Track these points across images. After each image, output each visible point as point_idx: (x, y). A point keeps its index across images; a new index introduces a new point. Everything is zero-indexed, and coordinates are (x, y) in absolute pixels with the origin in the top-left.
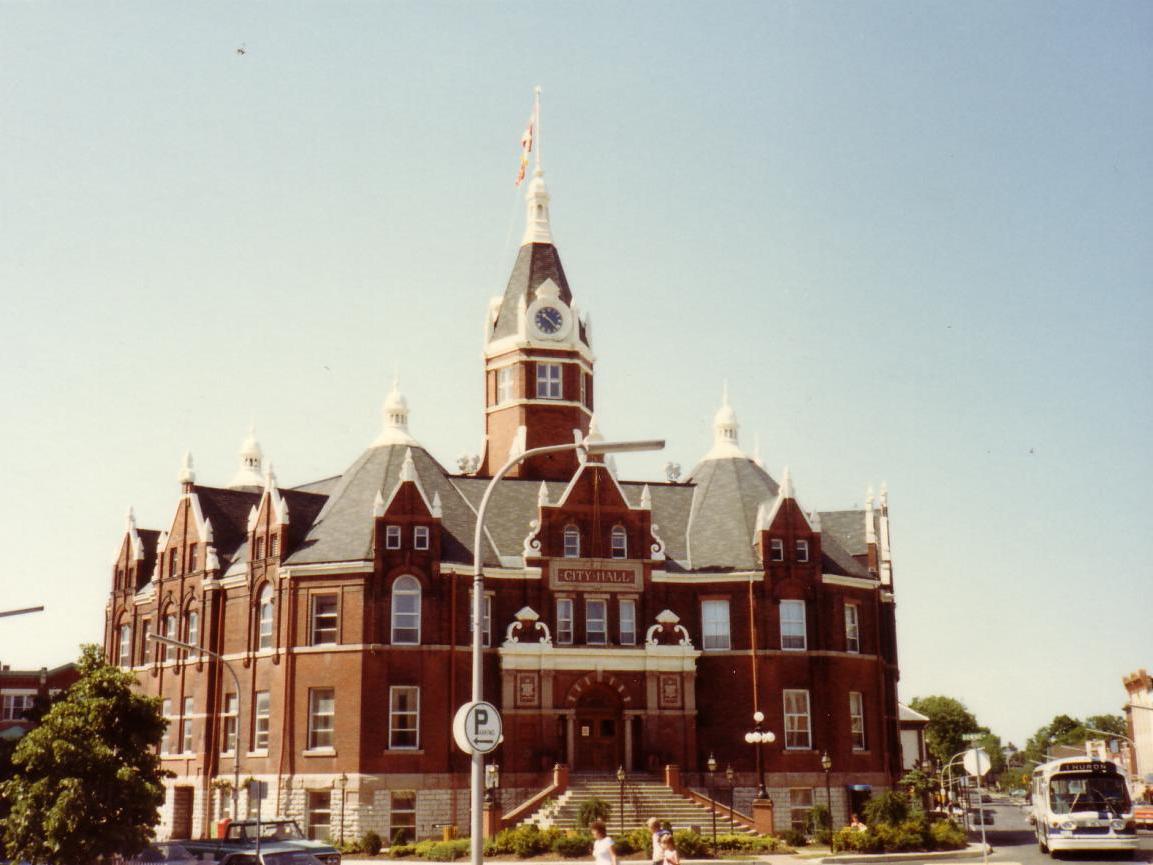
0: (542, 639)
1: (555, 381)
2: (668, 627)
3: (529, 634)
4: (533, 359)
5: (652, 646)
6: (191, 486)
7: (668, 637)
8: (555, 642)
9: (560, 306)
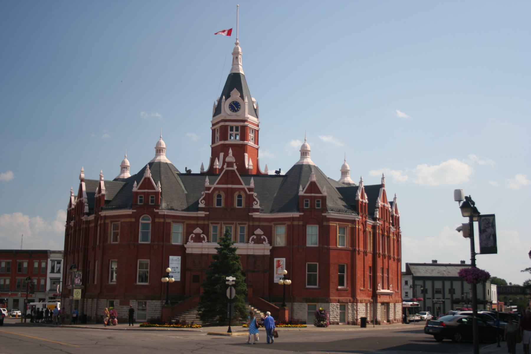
0: (203, 241)
1: (231, 132)
2: (259, 236)
3: (198, 239)
4: (227, 123)
6: (82, 180)
7: (259, 241)
9: (240, 100)
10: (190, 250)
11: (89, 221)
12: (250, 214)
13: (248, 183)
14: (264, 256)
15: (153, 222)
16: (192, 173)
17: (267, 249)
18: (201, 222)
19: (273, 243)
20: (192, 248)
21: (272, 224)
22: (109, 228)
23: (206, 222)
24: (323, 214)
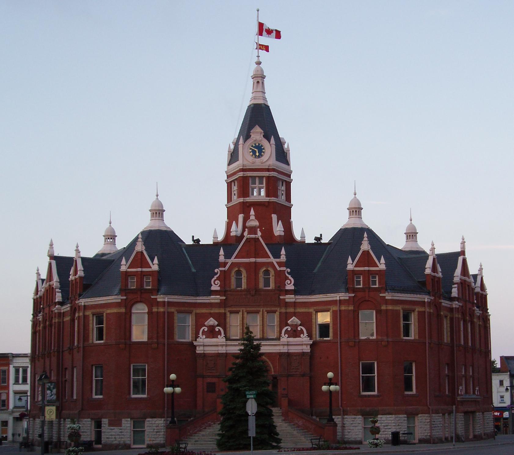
0: (219, 336)
3: (212, 333)
5: (285, 339)
6: (52, 257)
7: (295, 333)
8: (227, 339)
10: (201, 348)
11: (64, 312)
12: (281, 297)
13: (277, 255)
14: (303, 354)
15: (150, 313)
16: (201, 243)
17: (307, 345)
18: (216, 311)
19: (314, 336)
20: (204, 346)
21: (311, 310)
22: (91, 322)
23: (222, 311)
24: (381, 295)
